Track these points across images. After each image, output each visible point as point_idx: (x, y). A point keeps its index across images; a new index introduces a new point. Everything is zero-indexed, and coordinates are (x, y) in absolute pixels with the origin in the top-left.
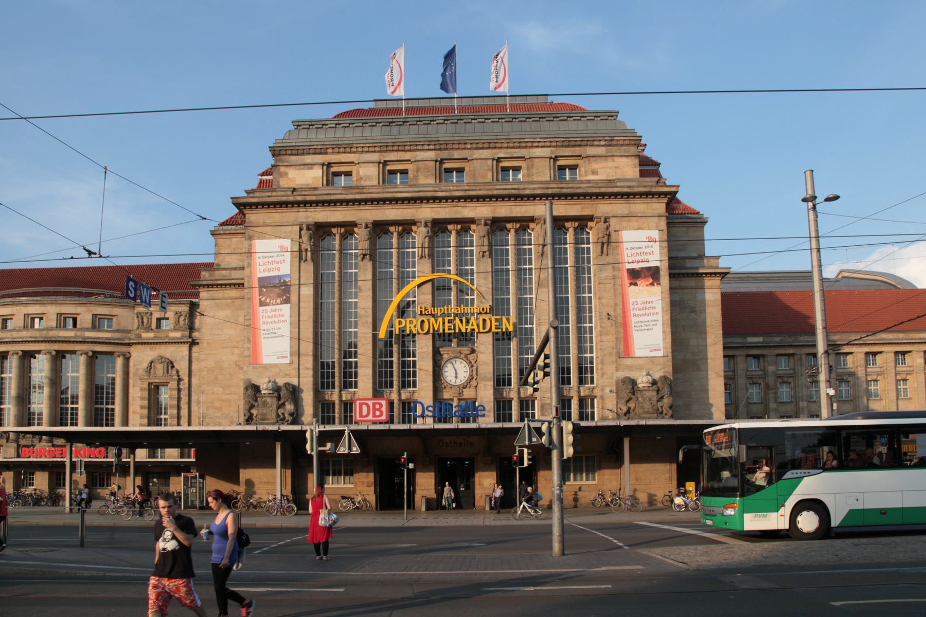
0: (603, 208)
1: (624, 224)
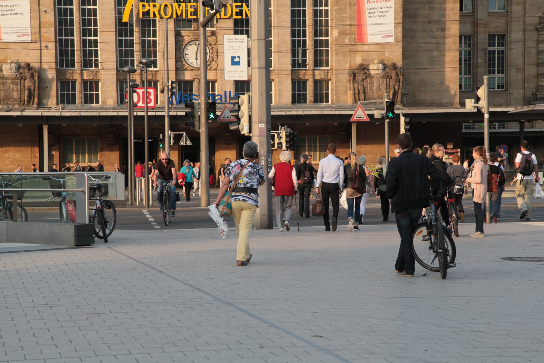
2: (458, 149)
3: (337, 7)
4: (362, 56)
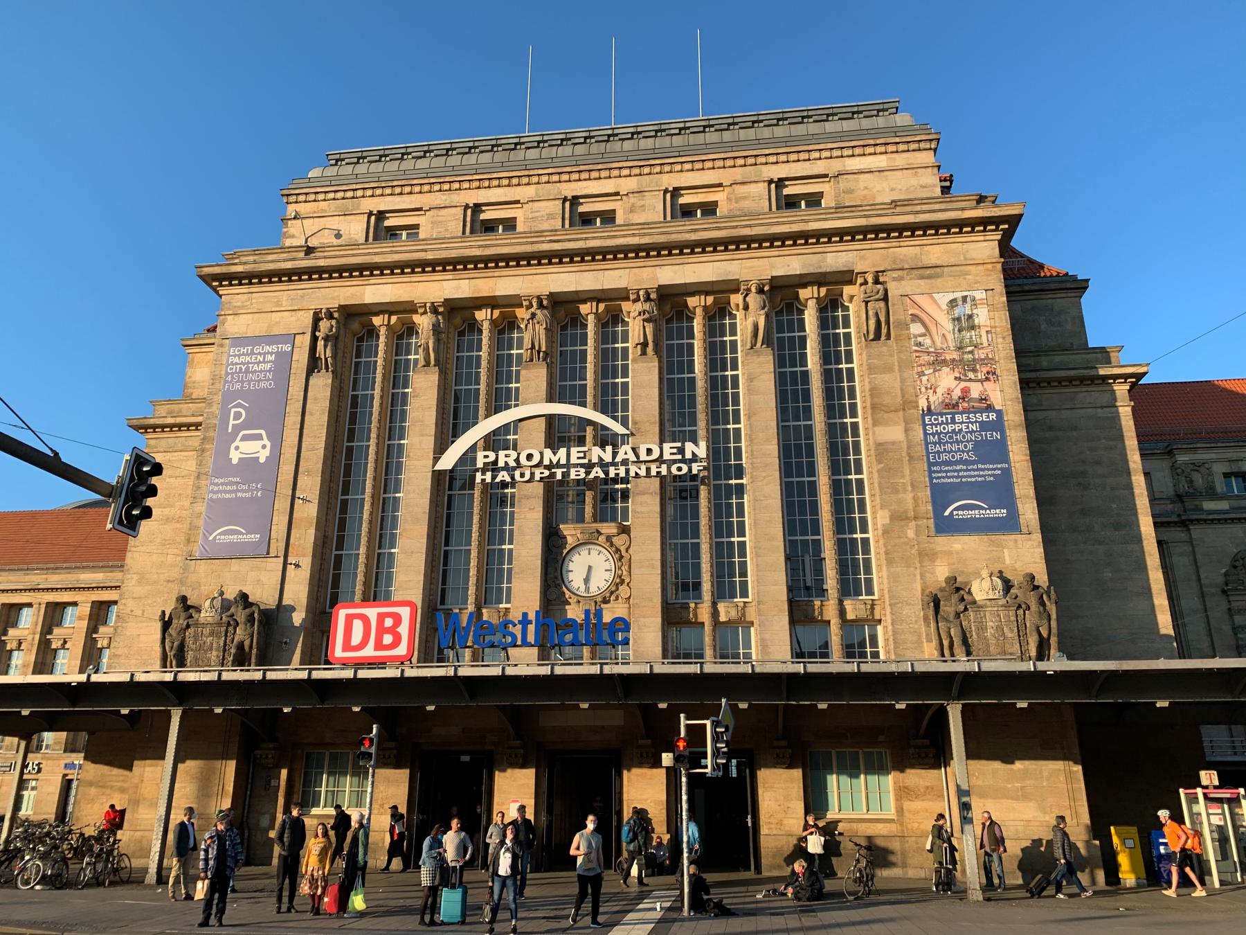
2: (1195, 788)
3: (882, 465)
4: (949, 564)
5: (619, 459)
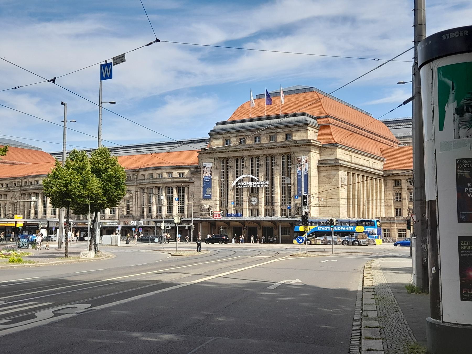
0: (293, 150)
1: (298, 154)
5: (257, 184)
